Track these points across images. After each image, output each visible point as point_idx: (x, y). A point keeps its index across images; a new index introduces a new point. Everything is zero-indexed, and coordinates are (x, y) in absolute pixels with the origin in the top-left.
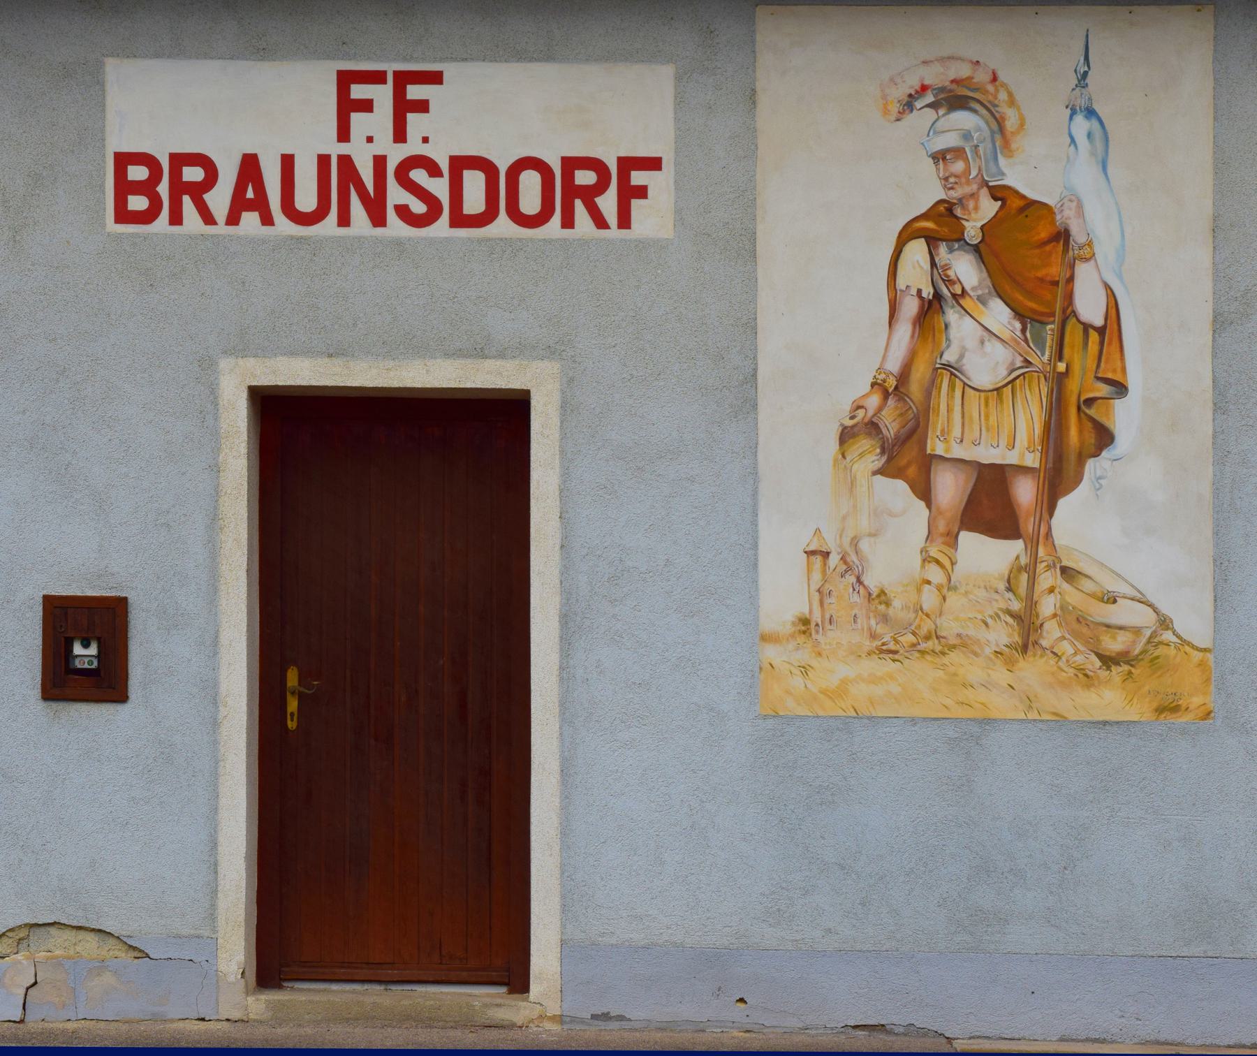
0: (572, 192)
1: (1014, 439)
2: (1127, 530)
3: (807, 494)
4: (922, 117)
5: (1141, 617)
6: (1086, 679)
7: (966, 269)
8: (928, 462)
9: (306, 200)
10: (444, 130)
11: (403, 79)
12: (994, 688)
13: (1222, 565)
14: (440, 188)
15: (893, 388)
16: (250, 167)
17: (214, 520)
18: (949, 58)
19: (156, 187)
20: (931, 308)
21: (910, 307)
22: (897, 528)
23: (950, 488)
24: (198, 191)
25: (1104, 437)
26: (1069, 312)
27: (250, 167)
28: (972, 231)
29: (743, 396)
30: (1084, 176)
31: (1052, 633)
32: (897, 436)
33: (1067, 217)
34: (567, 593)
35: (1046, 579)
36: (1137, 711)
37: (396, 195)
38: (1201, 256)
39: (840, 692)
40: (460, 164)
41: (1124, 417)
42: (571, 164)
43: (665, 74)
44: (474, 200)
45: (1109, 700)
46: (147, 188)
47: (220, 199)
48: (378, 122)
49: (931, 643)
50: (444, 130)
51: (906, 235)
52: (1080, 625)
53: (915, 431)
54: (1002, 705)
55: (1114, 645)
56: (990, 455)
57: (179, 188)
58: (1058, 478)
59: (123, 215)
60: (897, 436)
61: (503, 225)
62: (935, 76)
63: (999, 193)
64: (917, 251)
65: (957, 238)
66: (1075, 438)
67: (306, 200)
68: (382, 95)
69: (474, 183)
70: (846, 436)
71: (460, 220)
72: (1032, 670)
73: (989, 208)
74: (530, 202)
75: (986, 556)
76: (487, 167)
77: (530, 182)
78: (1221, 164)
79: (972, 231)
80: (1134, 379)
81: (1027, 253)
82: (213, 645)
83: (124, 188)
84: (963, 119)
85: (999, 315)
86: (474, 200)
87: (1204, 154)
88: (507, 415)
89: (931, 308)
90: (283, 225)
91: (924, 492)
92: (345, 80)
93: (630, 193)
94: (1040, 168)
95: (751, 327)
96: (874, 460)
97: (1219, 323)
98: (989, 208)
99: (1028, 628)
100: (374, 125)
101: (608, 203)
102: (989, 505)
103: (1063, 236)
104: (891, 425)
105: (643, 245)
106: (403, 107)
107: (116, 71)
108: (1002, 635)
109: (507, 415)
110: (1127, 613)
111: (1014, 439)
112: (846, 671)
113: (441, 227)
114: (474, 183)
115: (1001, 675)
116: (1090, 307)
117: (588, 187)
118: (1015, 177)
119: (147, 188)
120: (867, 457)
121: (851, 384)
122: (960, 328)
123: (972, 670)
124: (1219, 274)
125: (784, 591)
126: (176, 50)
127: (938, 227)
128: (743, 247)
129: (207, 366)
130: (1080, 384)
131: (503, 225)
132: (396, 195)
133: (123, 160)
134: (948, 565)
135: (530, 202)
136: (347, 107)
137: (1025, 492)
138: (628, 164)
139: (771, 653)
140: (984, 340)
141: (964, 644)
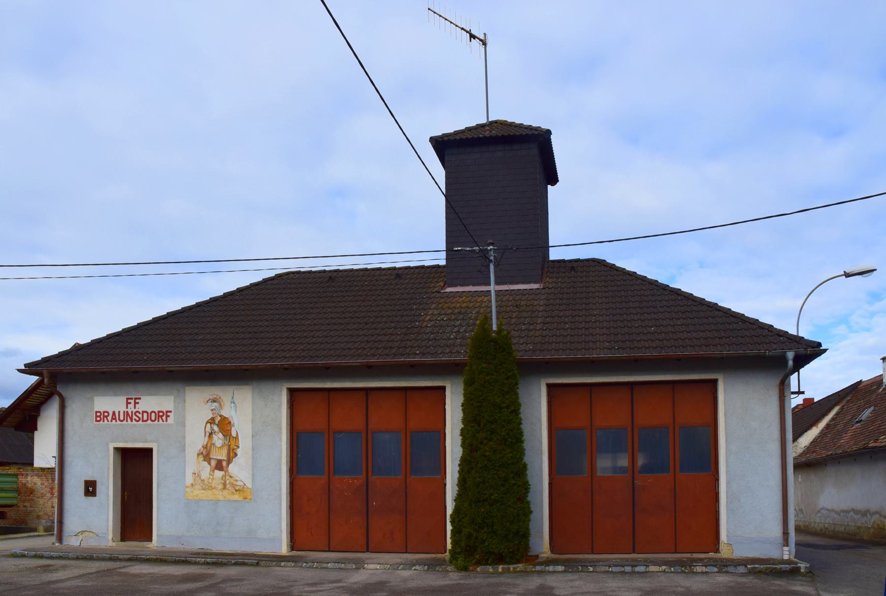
0: (159, 416)
1: (223, 455)
2: (239, 470)
3: (193, 465)
4: (210, 404)
5: (241, 484)
6: (233, 493)
7: (216, 428)
8: (210, 459)
9: (122, 418)
10: (141, 407)
11: (136, 399)
12: (220, 495)
13: (253, 475)
14: (140, 416)
15: (205, 447)
16: (114, 413)
17: (108, 468)
18: (130, 560)
19: (101, 416)
20: (211, 434)
21: (208, 434)
22: (206, 469)
23: (213, 463)
24: (107, 417)
25: (236, 455)
26: (231, 435)
27: (114, 413)
28: (217, 422)
29: (184, 450)
30: (233, 413)
31: (228, 486)
32: (206, 455)
33: (230, 419)
34: (158, 480)
35: (228, 477)
36: (241, 499)
37: (134, 417)
38: (250, 425)
39: (197, 496)
40: (143, 412)
41: (239, 451)
42: (159, 412)
43: (172, 398)
44: (145, 418)
45: (236, 497)
46: (100, 416)
47: (110, 418)
48: (131, 406)
49: (211, 488)
50: (141, 407)
51: (207, 423)
52: (232, 485)
53: (208, 454)
54: (221, 498)
55: (237, 488)
56: (219, 458)
57: (104, 416)
58: (229, 461)
59: (97, 421)
60: (206, 455)
61: (149, 421)
62: (212, 397)
63: (221, 416)
64: (209, 425)
65: (214, 423)
66: (232, 455)
67: (122, 418)
68: (132, 401)
69: (145, 415)
70: (198, 455)
71: (143, 421)
72: (225, 492)
73: (219, 418)
74: (153, 418)
75: (219, 474)
76: (147, 412)
77: (153, 414)
78: (253, 411)
79: (217, 422)
80: (240, 446)
81: (224, 425)
82: (108, 488)
83: (97, 416)
84: (215, 404)
85: (220, 435)
86: (145, 418)
87: (250, 410)
88: (149, 451)
89: (211, 434)
90: (119, 422)
91: (210, 464)
92: (127, 399)
93: (167, 416)
94: (227, 412)
95: (184, 437)
96: (202, 459)
97: (253, 436)
98: (219, 418)
99: (225, 485)
100: (131, 406)
101: (164, 418)
102: (219, 466)
103: (230, 423)
104: (205, 453)
105: (169, 425)
106: (136, 403)
107: (96, 398)
108: (221, 486)
109: (149, 451)
110: (239, 483)
111: (223, 455)
112: (198, 493)
113: (140, 422)
114: (145, 415)
115: (220, 493)
116: (234, 434)
117: (162, 415)
118: (223, 413)
119: (100, 416)
120: (201, 458)
121: (199, 447)
122: (215, 437)
123: (216, 492)
124: (253, 429)
125: (189, 479)
126: (104, 395)
127: (212, 421)
128: (183, 425)
129: (107, 444)
130: (233, 446)
131: (149, 421)
132: (134, 417)
133: (97, 412)
134: (213, 475)
135: (153, 418)
136: (128, 403)
137: (224, 464)
138: (167, 412)
139: (187, 489)
140: (218, 439)
141: (215, 488)
